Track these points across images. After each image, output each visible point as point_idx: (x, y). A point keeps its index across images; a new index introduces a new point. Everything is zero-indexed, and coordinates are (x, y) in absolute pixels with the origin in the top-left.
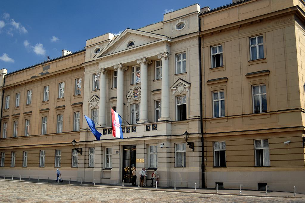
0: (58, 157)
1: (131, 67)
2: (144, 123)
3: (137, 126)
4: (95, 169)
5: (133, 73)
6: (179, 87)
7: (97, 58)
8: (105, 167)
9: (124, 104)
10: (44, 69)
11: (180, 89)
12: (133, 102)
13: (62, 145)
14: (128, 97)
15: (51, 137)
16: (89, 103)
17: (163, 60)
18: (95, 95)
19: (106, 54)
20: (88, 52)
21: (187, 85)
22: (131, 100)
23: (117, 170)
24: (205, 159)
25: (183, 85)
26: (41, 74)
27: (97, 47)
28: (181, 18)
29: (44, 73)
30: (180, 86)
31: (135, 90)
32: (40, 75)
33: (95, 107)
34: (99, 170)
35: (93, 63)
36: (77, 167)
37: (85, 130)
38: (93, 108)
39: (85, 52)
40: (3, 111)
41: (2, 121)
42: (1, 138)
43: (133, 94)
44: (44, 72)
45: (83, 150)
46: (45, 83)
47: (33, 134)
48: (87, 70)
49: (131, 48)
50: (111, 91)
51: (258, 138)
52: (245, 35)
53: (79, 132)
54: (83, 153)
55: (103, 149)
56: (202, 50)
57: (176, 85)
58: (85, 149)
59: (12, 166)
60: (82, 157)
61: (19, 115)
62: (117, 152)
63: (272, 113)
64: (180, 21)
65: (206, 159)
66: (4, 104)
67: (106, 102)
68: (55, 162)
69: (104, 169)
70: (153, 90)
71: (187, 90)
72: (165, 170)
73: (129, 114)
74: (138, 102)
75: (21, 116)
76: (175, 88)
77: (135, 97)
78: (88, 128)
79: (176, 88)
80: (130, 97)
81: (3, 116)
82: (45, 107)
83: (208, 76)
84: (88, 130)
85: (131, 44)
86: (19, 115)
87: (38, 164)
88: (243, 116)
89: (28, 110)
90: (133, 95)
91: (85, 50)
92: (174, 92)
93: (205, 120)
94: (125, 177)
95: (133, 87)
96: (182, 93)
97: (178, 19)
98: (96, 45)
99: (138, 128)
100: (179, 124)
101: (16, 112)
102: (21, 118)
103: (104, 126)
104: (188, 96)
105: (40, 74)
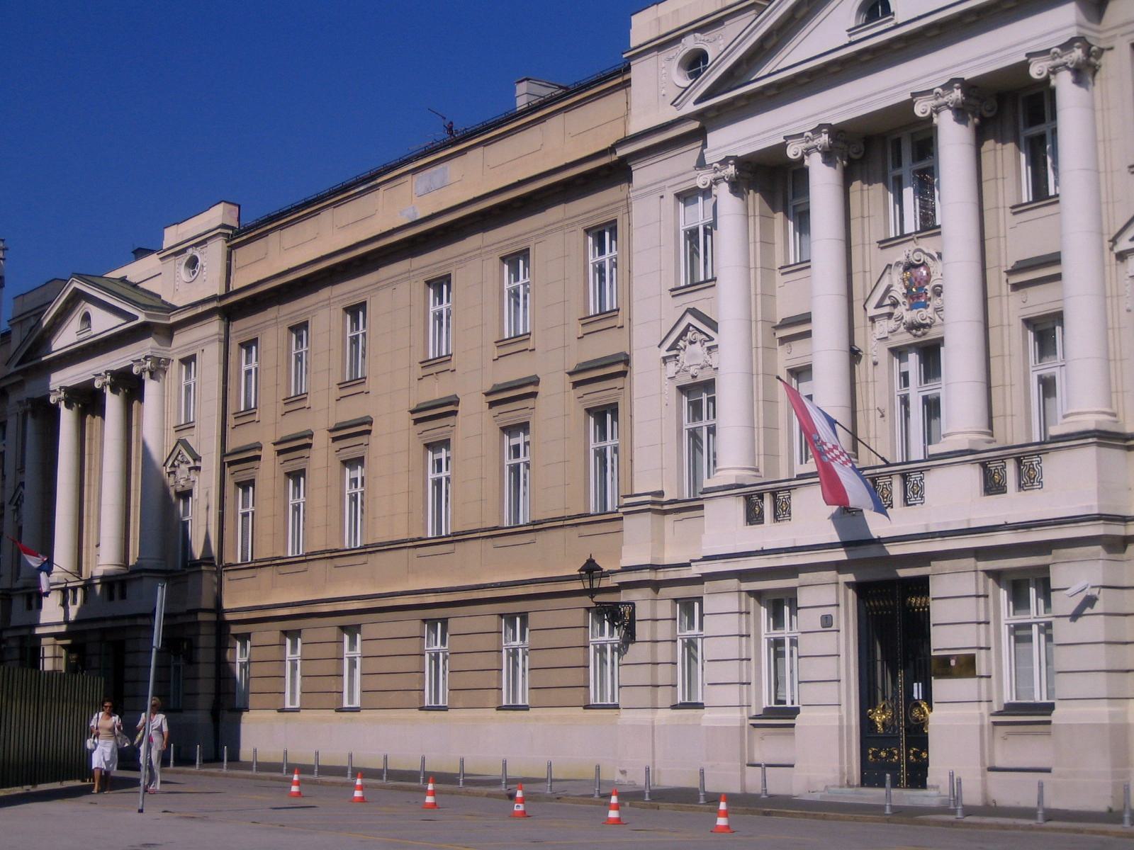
1: (882, 137)
2: (971, 452)
4: (707, 717)
5: (897, 172)
7: (690, 108)
8: (765, 704)
12: (905, 338)
14: (872, 312)
17: (1064, 84)
18: (694, 312)
20: (641, 72)
22: (892, 324)
23: (830, 717)
27: (690, 43)
31: (910, 266)
33: (694, 377)
34: (735, 717)
36: (616, 707)
37: (649, 506)
38: (686, 380)
39: (626, 77)
40: (231, 421)
41: (228, 471)
42: (230, 565)
43: (899, 291)
45: (642, 611)
47: (382, 535)
48: (643, 174)
53: (616, 516)
54: (642, 630)
58: (654, 609)
59: (288, 705)
61: (307, 441)
62: (827, 621)
66: (231, 385)
68: (500, 679)
69: (757, 717)
70: (1010, 264)
72: (1101, 712)
73: (883, 402)
74: (933, 334)
75: (321, 440)
77: (912, 308)
78: (661, 494)
80: (886, 310)
81: (228, 450)
82: (436, 390)
84: (662, 504)
86: (307, 441)
89: (351, 410)
90: (901, 299)
94: (876, 755)
95: (900, 254)
98: (683, 36)
99: (935, 482)
101: (293, 426)
102: (322, 456)
103: (747, 477)
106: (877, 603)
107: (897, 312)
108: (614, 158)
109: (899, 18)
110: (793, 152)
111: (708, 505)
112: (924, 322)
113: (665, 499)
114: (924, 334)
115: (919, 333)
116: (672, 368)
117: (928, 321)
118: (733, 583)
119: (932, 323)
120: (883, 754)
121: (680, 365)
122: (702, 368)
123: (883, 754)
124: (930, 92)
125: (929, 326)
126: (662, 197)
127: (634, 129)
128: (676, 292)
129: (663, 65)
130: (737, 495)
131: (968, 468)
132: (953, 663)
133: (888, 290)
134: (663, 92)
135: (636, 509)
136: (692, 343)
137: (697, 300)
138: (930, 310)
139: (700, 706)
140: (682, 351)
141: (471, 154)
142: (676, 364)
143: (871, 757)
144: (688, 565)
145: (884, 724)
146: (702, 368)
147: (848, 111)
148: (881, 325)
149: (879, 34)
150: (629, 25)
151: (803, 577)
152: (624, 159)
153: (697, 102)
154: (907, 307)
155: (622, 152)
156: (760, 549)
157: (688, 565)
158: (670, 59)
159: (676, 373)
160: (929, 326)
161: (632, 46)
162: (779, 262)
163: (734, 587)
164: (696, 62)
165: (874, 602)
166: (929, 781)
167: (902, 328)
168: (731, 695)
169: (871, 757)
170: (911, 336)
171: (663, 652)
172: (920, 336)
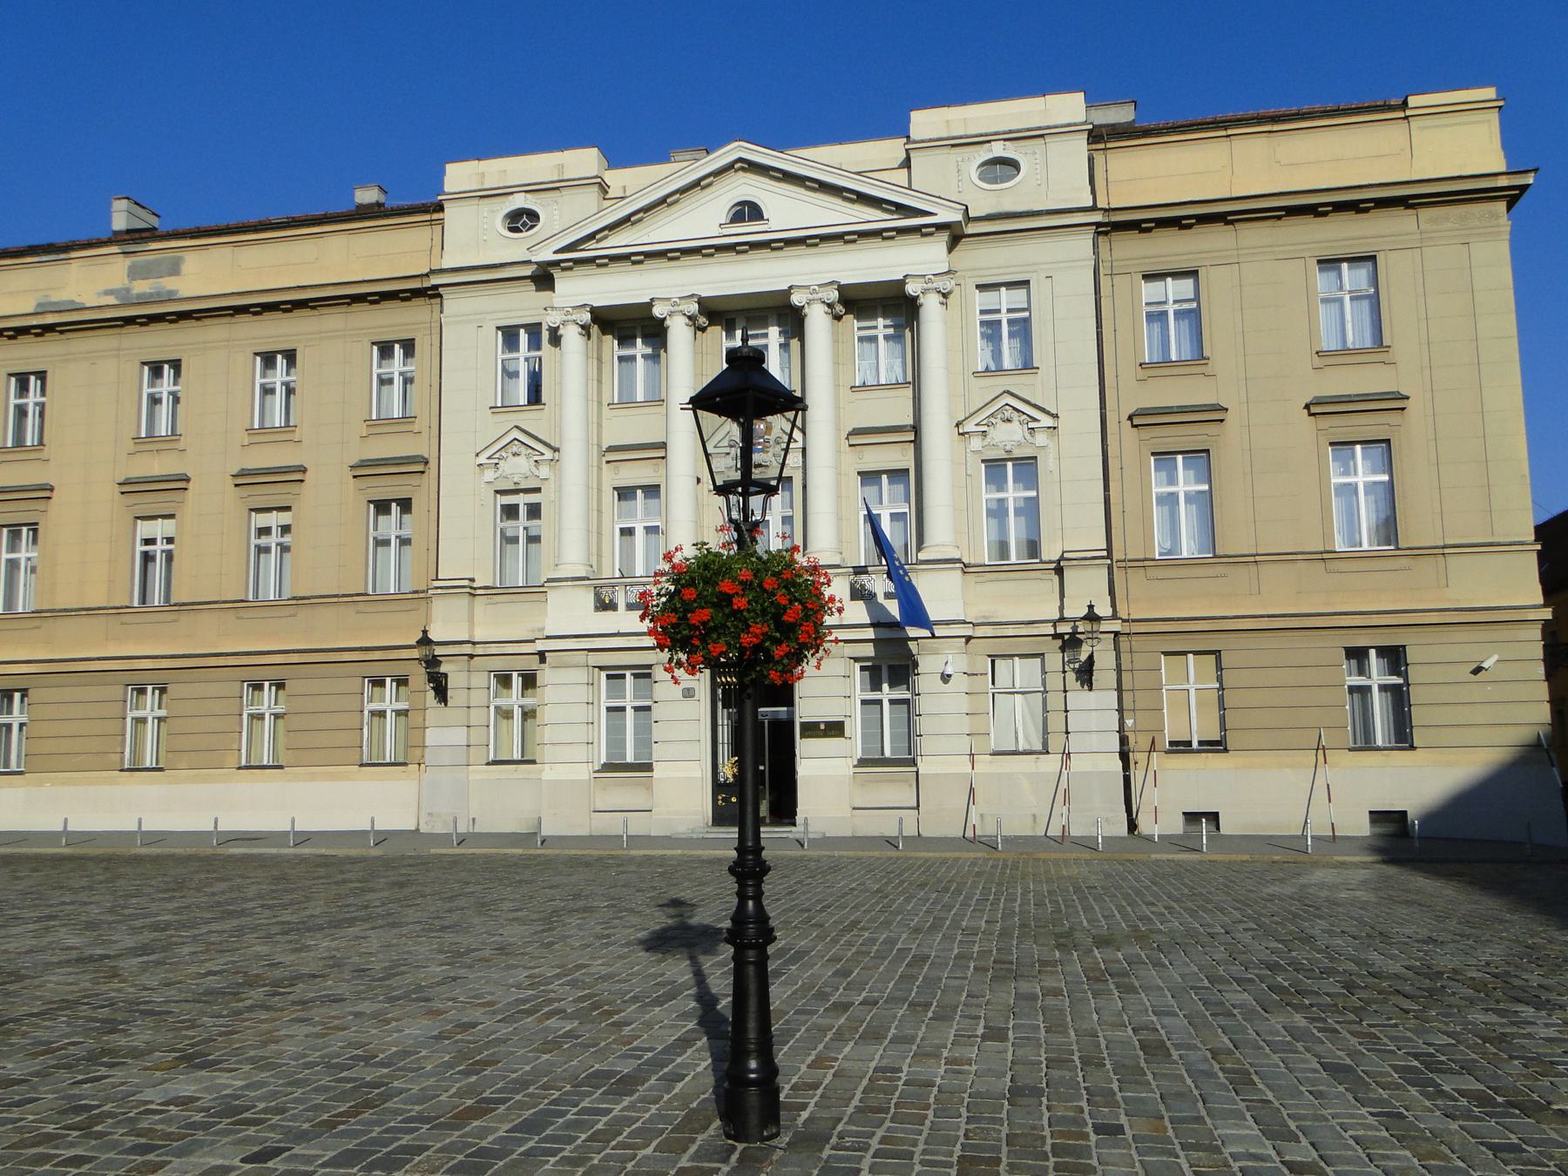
0: (143, 720)
4: (549, 773)
7: (547, 255)
10: (134, 274)
11: (1009, 436)
13: (295, 658)
15: (207, 619)
16: (482, 459)
19: (599, 241)
21: (1046, 421)
24: (1129, 722)
25: (1025, 416)
26: (117, 298)
27: (519, 201)
28: (1005, 140)
29: (135, 292)
32: (112, 300)
34: (583, 773)
35: (490, 277)
39: (435, 216)
44: (142, 287)
46: (159, 342)
48: (454, 303)
49: (748, 231)
51: (1361, 641)
52: (1303, 250)
56: (1105, 282)
57: (992, 415)
60: (451, 713)
63: (1418, 552)
64: (998, 150)
65: (1132, 721)
69: (598, 771)
71: (1041, 439)
78: (472, 580)
83: (1132, 395)
84: (475, 589)
85: (748, 211)
86: (47, 494)
87: (116, 757)
88: (1300, 557)
91: (440, 208)
92: (976, 443)
93: (1123, 564)
96: (1017, 453)
97: (989, 142)
100: (1003, 575)
104: (1046, 465)
105: (108, 293)
108: (426, 284)
109: (773, 225)
110: (658, 311)
111: (551, 595)
113: (475, 585)
116: (489, 475)
118: (580, 658)
121: (499, 472)
124: (808, 287)
127: (447, 263)
132: (822, 727)
134: (485, 237)
135: (450, 590)
136: (515, 454)
137: (533, 420)
138: (770, 454)
141: (213, 250)
144: (533, 641)
149: (748, 231)
150: (443, 173)
152: (436, 287)
153: (555, 252)
155: (435, 280)
157: (533, 641)
161: (446, 189)
162: (606, 400)
164: (521, 220)
166: (799, 818)
168: (581, 753)
171: (476, 717)
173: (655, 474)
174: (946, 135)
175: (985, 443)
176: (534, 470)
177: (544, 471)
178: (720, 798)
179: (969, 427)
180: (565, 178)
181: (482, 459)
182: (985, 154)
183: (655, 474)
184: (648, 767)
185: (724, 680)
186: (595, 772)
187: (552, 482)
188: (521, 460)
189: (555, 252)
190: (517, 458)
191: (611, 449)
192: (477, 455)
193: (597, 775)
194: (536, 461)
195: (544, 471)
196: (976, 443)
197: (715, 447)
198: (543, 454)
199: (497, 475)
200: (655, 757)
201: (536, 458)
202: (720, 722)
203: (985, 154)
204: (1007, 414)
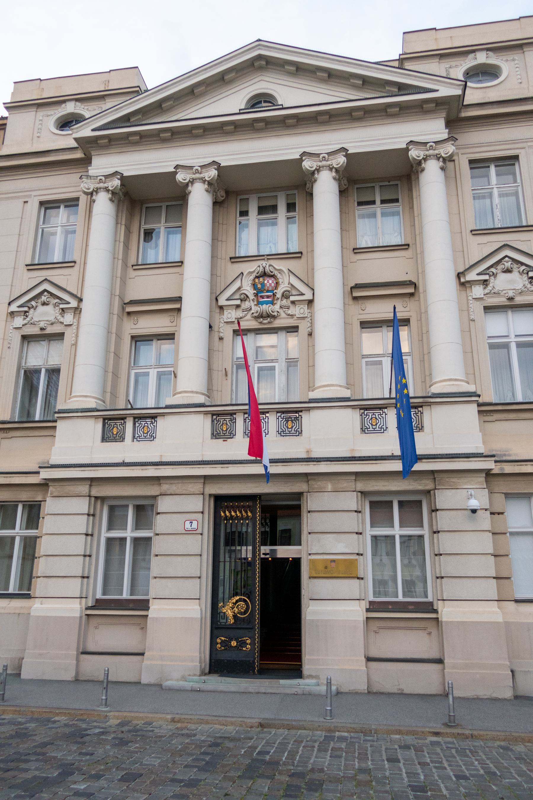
3: (309, 409)
6: (502, 277)
9: (210, 327)
14: (222, 301)
16: (14, 308)
25: (523, 267)
30: (508, 271)
31: (264, 274)
33: (42, 329)
43: (250, 292)
50: (132, 273)
55: (95, 508)
57: (492, 266)
64: (482, 58)
67: (111, 313)
70: (353, 285)
76: (486, 277)
77: (258, 303)
79: (490, 276)
80: (238, 302)
90: (251, 297)
92: (478, 291)
106: (233, 514)
107: (246, 305)
111: (60, 425)
112: (273, 314)
114: (269, 323)
115: (265, 321)
116: (19, 321)
117: (275, 314)
118: (84, 489)
119: (278, 316)
120: (234, 643)
121: (28, 319)
122: (52, 324)
123: (234, 643)
125: (274, 317)
126: (26, 202)
128: (31, 267)
129: (41, 118)
130: (96, 417)
131: (349, 411)
133: (239, 288)
134: (39, 135)
136: (44, 304)
138: (277, 307)
139: (28, 596)
140: (32, 310)
142: (25, 319)
143: (219, 646)
145: (235, 616)
146: (52, 324)
147: (233, 159)
148: (230, 313)
151: (165, 487)
153: (93, 130)
154: (255, 303)
156: (121, 461)
158: (48, 116)
159: (23, 325)
160: (274, 317)
163: (84, 493)
165: (230, 512)
166: (307, 668)
167: (249, 317)
169: (219, 646)
170: (258, 324)
172: (264, 324)
173: (171, 324)
174: (435, 48)
175: (487, 291)
176: (59, 317)
177: (68, 318)
178: (219, 641)
179: (472, 276)
180: (110, 88)
181: (14, 308)
182: (469, 62)
183: (171, 324)
184: (144, 605)
185: (227, 513)
186: (87, 609)
187: (74, 327)
188: (49, 309)
189: (93, 130)
190: (45, 307)
191: (133, 303)
192: (9, 304)
193: (89, 612)
194: (63, 309)
195: (68, 318)
196: (478, 291)
197: (227, 300)
198: (69, 303)
199: (25, 322)
200: (152, 594)
201: (62, 306)
202: (222, 559)
203: (469, 62)
204: (508, 264)
